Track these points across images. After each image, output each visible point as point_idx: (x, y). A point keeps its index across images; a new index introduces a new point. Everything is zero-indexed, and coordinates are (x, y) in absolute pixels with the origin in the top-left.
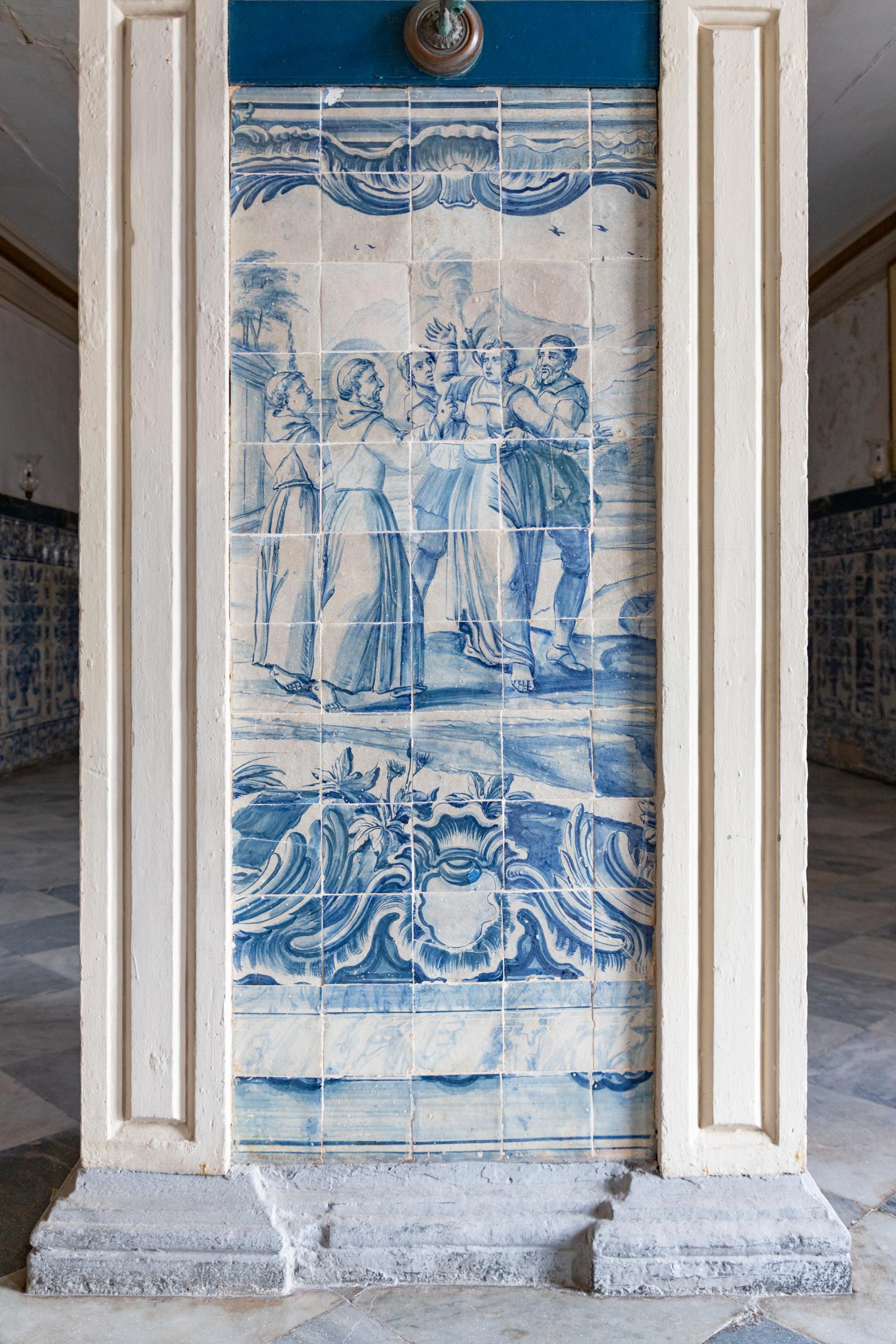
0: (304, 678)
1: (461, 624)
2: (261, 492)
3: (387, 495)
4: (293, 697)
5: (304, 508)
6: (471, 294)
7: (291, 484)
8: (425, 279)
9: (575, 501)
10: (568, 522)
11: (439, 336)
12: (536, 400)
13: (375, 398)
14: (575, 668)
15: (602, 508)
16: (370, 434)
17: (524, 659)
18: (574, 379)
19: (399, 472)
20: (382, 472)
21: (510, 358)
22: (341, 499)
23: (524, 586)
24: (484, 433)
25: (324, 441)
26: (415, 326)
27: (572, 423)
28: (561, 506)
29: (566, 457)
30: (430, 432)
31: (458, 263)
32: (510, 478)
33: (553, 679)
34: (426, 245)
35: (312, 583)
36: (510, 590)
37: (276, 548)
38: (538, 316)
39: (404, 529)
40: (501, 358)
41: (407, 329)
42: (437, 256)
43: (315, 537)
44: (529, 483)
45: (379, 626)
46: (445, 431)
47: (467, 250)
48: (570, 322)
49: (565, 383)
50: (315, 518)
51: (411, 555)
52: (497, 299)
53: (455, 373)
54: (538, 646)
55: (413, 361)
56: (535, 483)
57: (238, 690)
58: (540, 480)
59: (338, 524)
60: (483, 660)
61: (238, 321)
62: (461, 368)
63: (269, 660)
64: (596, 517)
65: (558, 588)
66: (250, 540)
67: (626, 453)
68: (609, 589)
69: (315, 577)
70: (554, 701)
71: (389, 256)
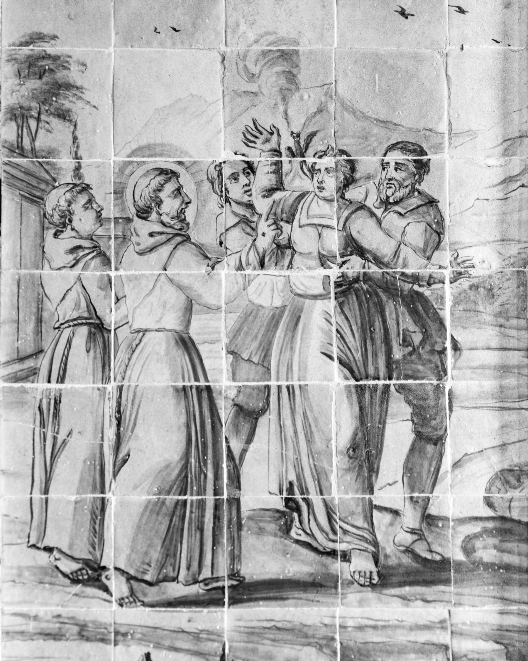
0: (92, 564)
1: (287, 500)
2: (38, 332)
3: (194, 338)
4: (78, 588)
5: (92, 352)
6: (298, 89)
7: (76, 323)
8: (241, 71)
9: (428, 348)
10: (419, 375)
11: (259, 142)
12: (379, 222)
13: (180, 216)
14: (429, 557)
15: (462, 357)
16: (173, 261)
17: (366, 545)
18: (427, 196)
19: (209, 308)
20: (189, 309)
21: (347, 170)
22: (137, 341)
23: (365, 454)
24: (315, 262)
25: (116, 269)
26: (229, 128)
27: (424, 251)
28: (411, 354)
29: (417, 293)
30: (247, 259)
31: (283, 51)
32: (347, 318)
33: (401, 570)
34: (243, 28)
35: (102, 446)
36: (347, 459)
37: (57, 402)
38: (382, 117)
39: (216, 381)
40: (336, 169)
41: (219, 132)
42: (256, 42)
43: (105, 388)
44: (372, 325)
45: (185, 501)
46: (267, 260)
47: (293, 35)
48: (421, 126)
49: (415, 201)
50: (105, 364)
51: (225, 413)
52: (331, 97)
53: (279, 187)
54: (383, 528)
55: (227, 171)
56: (378, 324)
57: (9, 578)
58: (384, 321)
59: (133, 373)
60: (315, 544)
61: (11, 119)
62: (286, 181)
63: (48, 542)
64: (454, 368)
65: (408, 457)
66: (25, 391)
67: (490, 290)
68: (471, 460)
69: (105, 438)
70: (403, 598)
71: (197, 42)
